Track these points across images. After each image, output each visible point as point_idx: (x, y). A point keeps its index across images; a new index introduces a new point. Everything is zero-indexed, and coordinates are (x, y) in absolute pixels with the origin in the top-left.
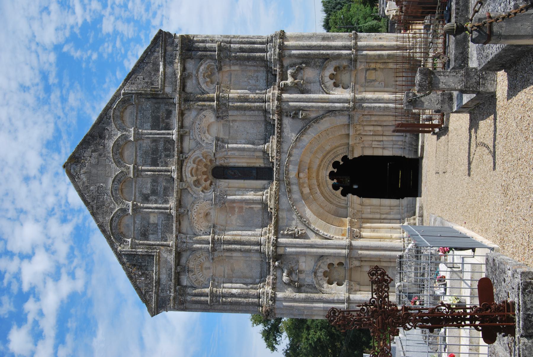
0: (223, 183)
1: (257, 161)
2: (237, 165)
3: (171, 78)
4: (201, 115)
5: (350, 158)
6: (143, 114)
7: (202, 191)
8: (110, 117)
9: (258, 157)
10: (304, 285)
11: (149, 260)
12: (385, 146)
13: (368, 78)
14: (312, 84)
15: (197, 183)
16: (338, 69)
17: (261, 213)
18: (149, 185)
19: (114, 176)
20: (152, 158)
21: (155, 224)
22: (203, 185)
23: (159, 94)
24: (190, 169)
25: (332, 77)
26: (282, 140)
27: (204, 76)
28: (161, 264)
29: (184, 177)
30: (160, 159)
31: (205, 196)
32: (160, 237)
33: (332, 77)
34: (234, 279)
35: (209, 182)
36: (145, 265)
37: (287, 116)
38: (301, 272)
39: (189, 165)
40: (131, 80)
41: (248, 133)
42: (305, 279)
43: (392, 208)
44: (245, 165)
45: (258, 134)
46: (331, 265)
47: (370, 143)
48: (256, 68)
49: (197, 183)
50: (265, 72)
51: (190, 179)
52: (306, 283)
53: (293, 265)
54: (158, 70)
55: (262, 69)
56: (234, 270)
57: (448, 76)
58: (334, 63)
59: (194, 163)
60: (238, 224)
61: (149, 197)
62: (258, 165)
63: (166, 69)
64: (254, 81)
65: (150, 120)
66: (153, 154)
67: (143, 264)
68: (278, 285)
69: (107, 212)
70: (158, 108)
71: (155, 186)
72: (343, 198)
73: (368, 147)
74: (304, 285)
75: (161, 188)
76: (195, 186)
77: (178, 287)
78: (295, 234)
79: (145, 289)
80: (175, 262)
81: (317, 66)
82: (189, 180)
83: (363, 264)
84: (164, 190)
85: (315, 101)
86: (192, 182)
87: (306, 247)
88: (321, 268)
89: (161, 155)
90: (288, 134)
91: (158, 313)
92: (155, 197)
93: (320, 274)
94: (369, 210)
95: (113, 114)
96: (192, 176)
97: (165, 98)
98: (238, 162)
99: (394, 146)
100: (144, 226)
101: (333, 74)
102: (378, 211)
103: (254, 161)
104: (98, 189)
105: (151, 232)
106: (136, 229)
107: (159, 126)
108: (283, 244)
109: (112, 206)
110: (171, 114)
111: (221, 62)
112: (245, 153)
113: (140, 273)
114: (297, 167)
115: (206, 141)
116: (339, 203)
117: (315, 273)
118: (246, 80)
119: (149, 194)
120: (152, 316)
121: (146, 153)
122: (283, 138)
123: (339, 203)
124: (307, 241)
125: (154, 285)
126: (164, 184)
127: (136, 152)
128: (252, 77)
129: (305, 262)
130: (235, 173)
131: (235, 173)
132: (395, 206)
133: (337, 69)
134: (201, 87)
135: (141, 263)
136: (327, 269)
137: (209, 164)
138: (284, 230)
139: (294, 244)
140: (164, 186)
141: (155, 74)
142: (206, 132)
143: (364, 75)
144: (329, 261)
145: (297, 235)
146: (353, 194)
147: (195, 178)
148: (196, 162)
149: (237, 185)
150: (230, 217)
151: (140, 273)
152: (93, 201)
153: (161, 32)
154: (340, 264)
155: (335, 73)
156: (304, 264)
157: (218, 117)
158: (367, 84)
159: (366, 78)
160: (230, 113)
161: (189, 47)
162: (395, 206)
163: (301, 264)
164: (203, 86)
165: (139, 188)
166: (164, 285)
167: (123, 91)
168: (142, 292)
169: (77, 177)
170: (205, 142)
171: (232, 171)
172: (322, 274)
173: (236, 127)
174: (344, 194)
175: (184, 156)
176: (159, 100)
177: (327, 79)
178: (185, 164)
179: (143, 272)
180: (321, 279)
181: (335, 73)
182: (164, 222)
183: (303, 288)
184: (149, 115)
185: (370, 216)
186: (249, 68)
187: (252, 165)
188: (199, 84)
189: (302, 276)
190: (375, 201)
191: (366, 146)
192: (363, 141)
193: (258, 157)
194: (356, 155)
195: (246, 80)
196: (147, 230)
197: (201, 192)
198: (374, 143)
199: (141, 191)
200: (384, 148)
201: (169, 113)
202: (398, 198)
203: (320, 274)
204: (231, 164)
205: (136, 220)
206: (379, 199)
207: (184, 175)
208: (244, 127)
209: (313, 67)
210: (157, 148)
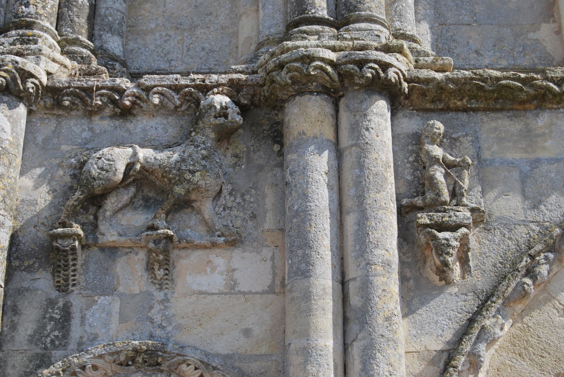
10: (63, 288)
38: (162, 256)
52: (76, 300)
53: (207, 208)
68: (76, 127)
74: (63, 288)
78: (436, 205)
87: (343, 282)
108: (357, 130)
124: (388, 287)
129: (232, 289)
138: (449, 141)
139: (361, 198)
145: (424, 218)
156: (215, 281)
163: (219, 260)
183: (43, 282)
189: (131, 274)
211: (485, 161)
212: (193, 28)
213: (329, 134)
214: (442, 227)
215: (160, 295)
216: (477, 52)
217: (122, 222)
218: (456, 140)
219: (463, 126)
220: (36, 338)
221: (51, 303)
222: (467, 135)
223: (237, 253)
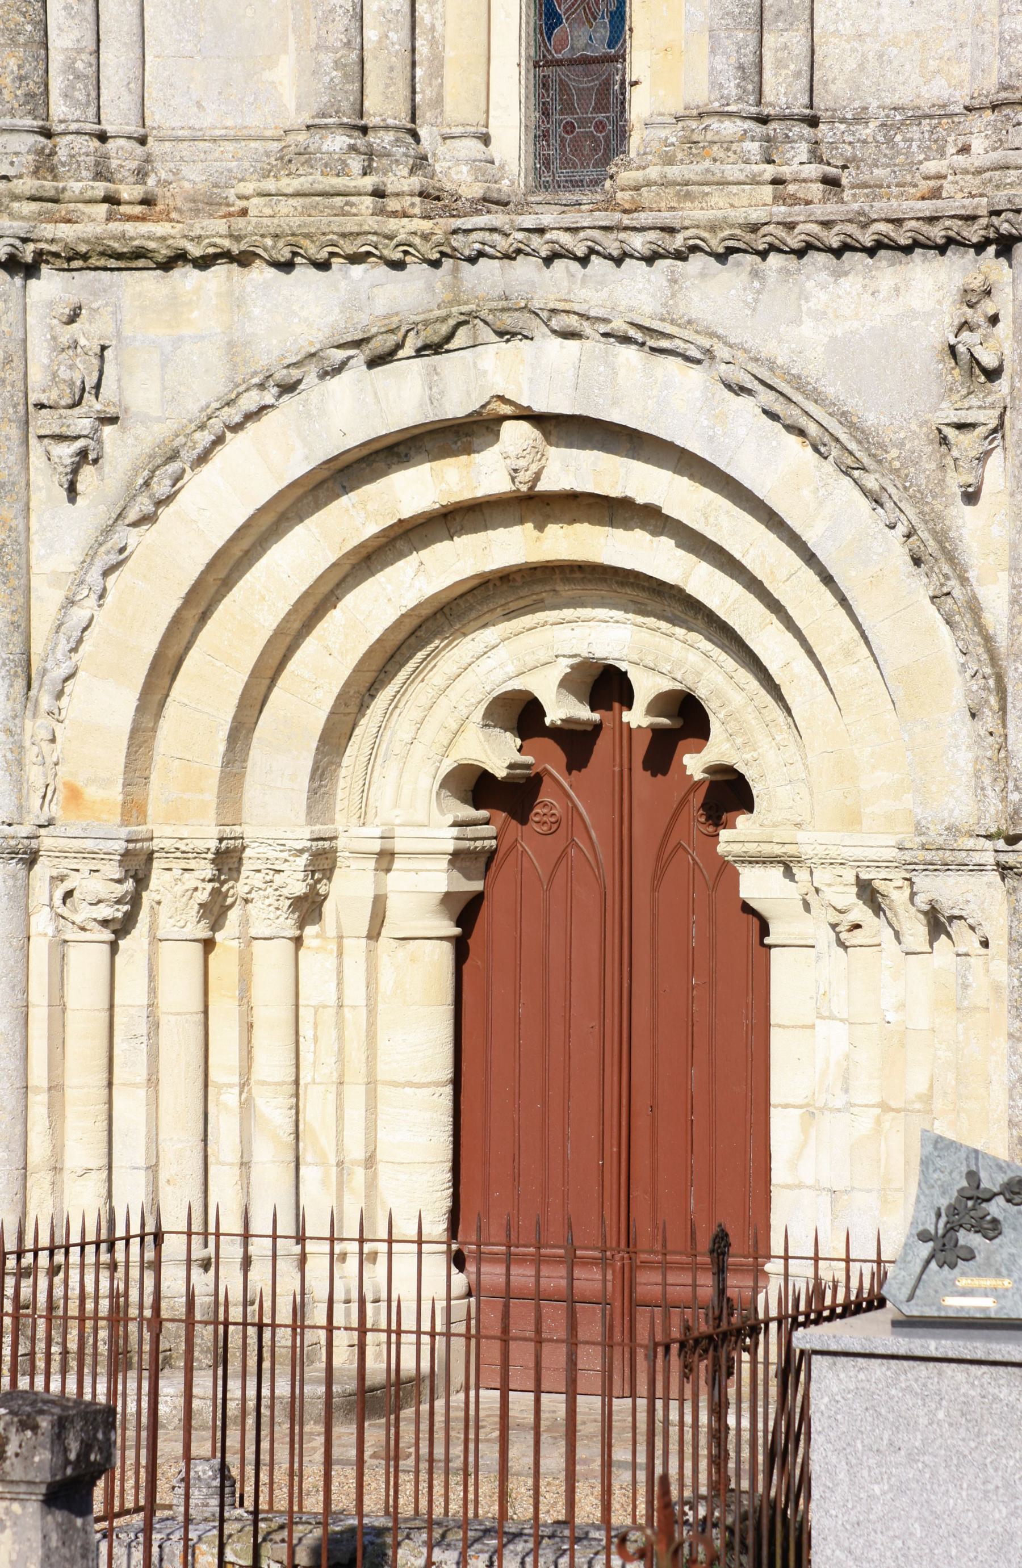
5: (738, 836)
17: (254, 121)
37: (971, 298)
45: (871, 47)
90: (819, 316)
211: (126, 338)
216: (199, 105)
218: (96, 310)
219: (105, 291)
222: (107, 305)
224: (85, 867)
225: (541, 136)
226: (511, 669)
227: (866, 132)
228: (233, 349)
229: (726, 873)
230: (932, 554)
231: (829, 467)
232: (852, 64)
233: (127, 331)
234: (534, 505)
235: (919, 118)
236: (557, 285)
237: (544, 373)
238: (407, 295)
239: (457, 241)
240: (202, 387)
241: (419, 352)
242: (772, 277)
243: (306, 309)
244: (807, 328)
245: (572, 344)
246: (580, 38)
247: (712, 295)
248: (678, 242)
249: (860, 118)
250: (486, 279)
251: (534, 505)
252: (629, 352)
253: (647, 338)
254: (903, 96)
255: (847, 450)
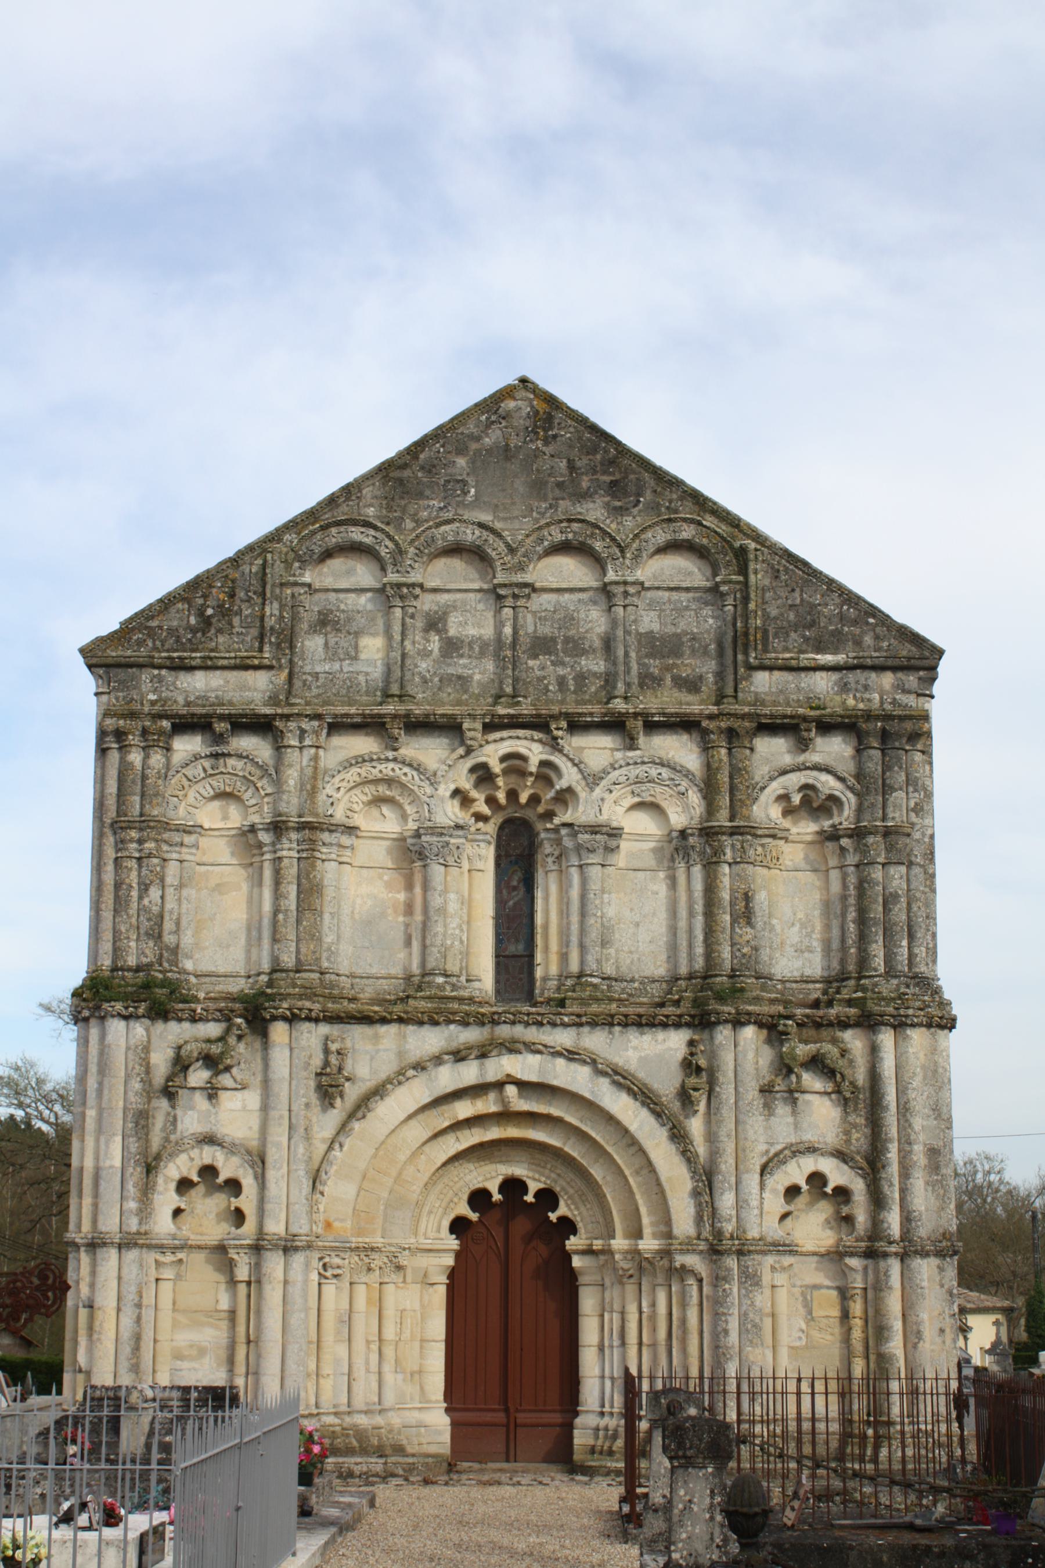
0: (482, 856)
1: (554, 958)
2: (539, 894)
3: (799, 689)
4: (685, 783)
5: (572, 1243)
6: (687, 608)
7: (457, 792)
8: (676, 512)
9: (564, 957)
10: (173, 1107)
11: (248, 639)
12: (607, 1351)
13: (816, 1293)
14: (790, 1120)
15: (483, 775)
16: (840, 1199)
18: (472, 631)
19: (498, 525)
20: (553, 640)
21: (357, 652)
22: (474, 794)
23: (746, 653)
24: (523, 751)
25: (817, 1179)
26: (617, 1029)
27: (806, 787)
28: (235, 673)
29: (497, 735)
30: (553, 663)
31: (442, 799)
32: (318, 669)
33: (817, 1179)
34: (193, 892)
35: (485, 810)
36: (233, 627)
37: (691, 1043)
38: (212, 1093)
39: (537, 748)
40: (786, 569)
41: (637, 925)
42: (192, 1108)
43: (417, 1377)
44: (539, 919)
45: (636, 956)
46: (234, 1186)
47: (616, 1307)
48: (836, 945)
49: (483, 775)
50: (826, 974)
51: (493, 752)
54: (819, 650)
55: (835, 964)
56: (221, 893)
57: (712, 1518)
58: (858, 1187)
59: (544, 764)
60: (359, 901)
61: (439, 632)
62: (539, 958)
63: (824, 674)
64: (796, 939)
65: (670, 630)
66: (567, 640)
67: (236, 621)
69: (389, 508)
70: (706, 652)
71: (471, 648)
72: (446, 1224)
73: (603, 1299)
74: (173, 1107)
75: (465, 666)
76: (473, 770)
77: (166, 724)
79: (160, 628)
80: (242, 716)
81: (847, 1133)
82: (489, 749)
83: (242, 1289)
84: (459, 677)
85: (740, 1128)
86: (483, 759)
88: (227, 1160)
89: (563, 664)
90: (635, 1048)
91: (90, 667)
92: (436, 651)
93: (208, 1155)
94: (408, 1305)
95: (684, 520)
96: (504, 759)
97: (736, 673)
98: (546, 899)
99: (608, 1383)
100: (349, 620)
101: (825, 1183)
102: (407, 1335)
103: (554, 946)
104: (458, 481)
105: (332, 642)
106: (342, 596)
107: (651, 655)
109: (409, 524)
110: (689, 691)
111: (850, 836)
112: (575, 919)
113: (210, 612)
114: (533, 1078)
115: (610, 798)
116: (430, 1212)
117: (209, 1140)
118: (800, 915)
119: (446, 631)
120: (82, 651)
121: (570, 619)
122: (621, 1032)
123: (430, 1212)
125: (175, 655)
126: (477, 677)
127: (571, 590)
128: (809, 935)
129: (244, 1109)
130: (515, 888)
131: (515, 888)
132: (422, 1388)
133: (842, 1194)
134: (772, 779)
135: (239, 612)
136: (221, 1179)
137: (541, 809)
140: (471, 677)
141: (807, 640)
142: (637, 800)
143: (827, 1283)
144: (248, 1183)
146: (458, 1255)
147: (497, 768)
148: (546, 771)
149: (477, 896)
150: (380, 878)
151: (210, 612)
152: (422, 468)
153: (941, 653)
154: (239, 1217)
155: (829, 1190)
157: (683, 834)
158: (797, 1291)
159: (816, 1287)
160: (697, 871)
161: (895, 738)
162: (422, 1388)
163: (239, 1095)
164: (774, 785)
165: (464, 603)
166: (174, 683)
167: (753, 545)
168: (152, 617)
169: (493, 418)
170: (606, 795)
171: (519, 882)
172: (207, 1161)
173: (655, 888)
174: (458, 1226)
175: (560, 733)
176: (729, 652)
177: (809, 1164)
178: (537, 735)
179: (214, 620)
180: (192, 1159)
181: (829, 1190)
182: (361, 678)
184: (682, 626)
185: (390, 1312)
186: (836, 924)
187: (539, 940)
188: (784, 772)
189: (200, 1101)
190: (437, 1326)
191: (607, 1294)
192: (622, 1283)
193: (564, 957)
194: (577, 1262)
195: (800, 915)
196: (338, 630)
197: (452, 787)
198: (616, 1316)
199: (455, 608)
200: (601, 1348)
201: (692, 685)
202: (449, 1394)
203: (208, 1155)
204: (540, 876)
205: (369, 595)
206: (443, 1337)
207: (505, 734)
208: (654, 914)
209: (844, 1120)
210: (584, 652)
212: (228, 946)
213: (287, 1041)
214: (331, 1086)
215: (213, 1111)
217: (199, 1076)
220: (164, 1129)
221: (169, 1114)
223: (246, 1092)
224: (333, 1254)
225: (497, 981)
226: (480, 1179)
227: (636, 985)
228: (401, 1054)
229: (567, 1257)
230: (678, 1136)
231: (638, 1104)
232: (628, 961)
233: (357, 1047)
234: (506, 1116)
235: (654, 981)
236: (532, 1034)
237: (525, 1066)
238: (472, 1035)
239: (496, 1017)
240: (386, 1068)
241: (477, 1058)
242: (617, 1034)
243: (428, 1040)
244: (630, 1053)
245: (538, 1057)
246: (516, 948)
247: (595, 1041)
248: (584, 1019)
249: (633, 980)
250: (504, 1031)
251: (506, 1116)
252: (561, 1062)
253: (571, 1055)
254: (647, 973)
255: (645, 1096)
